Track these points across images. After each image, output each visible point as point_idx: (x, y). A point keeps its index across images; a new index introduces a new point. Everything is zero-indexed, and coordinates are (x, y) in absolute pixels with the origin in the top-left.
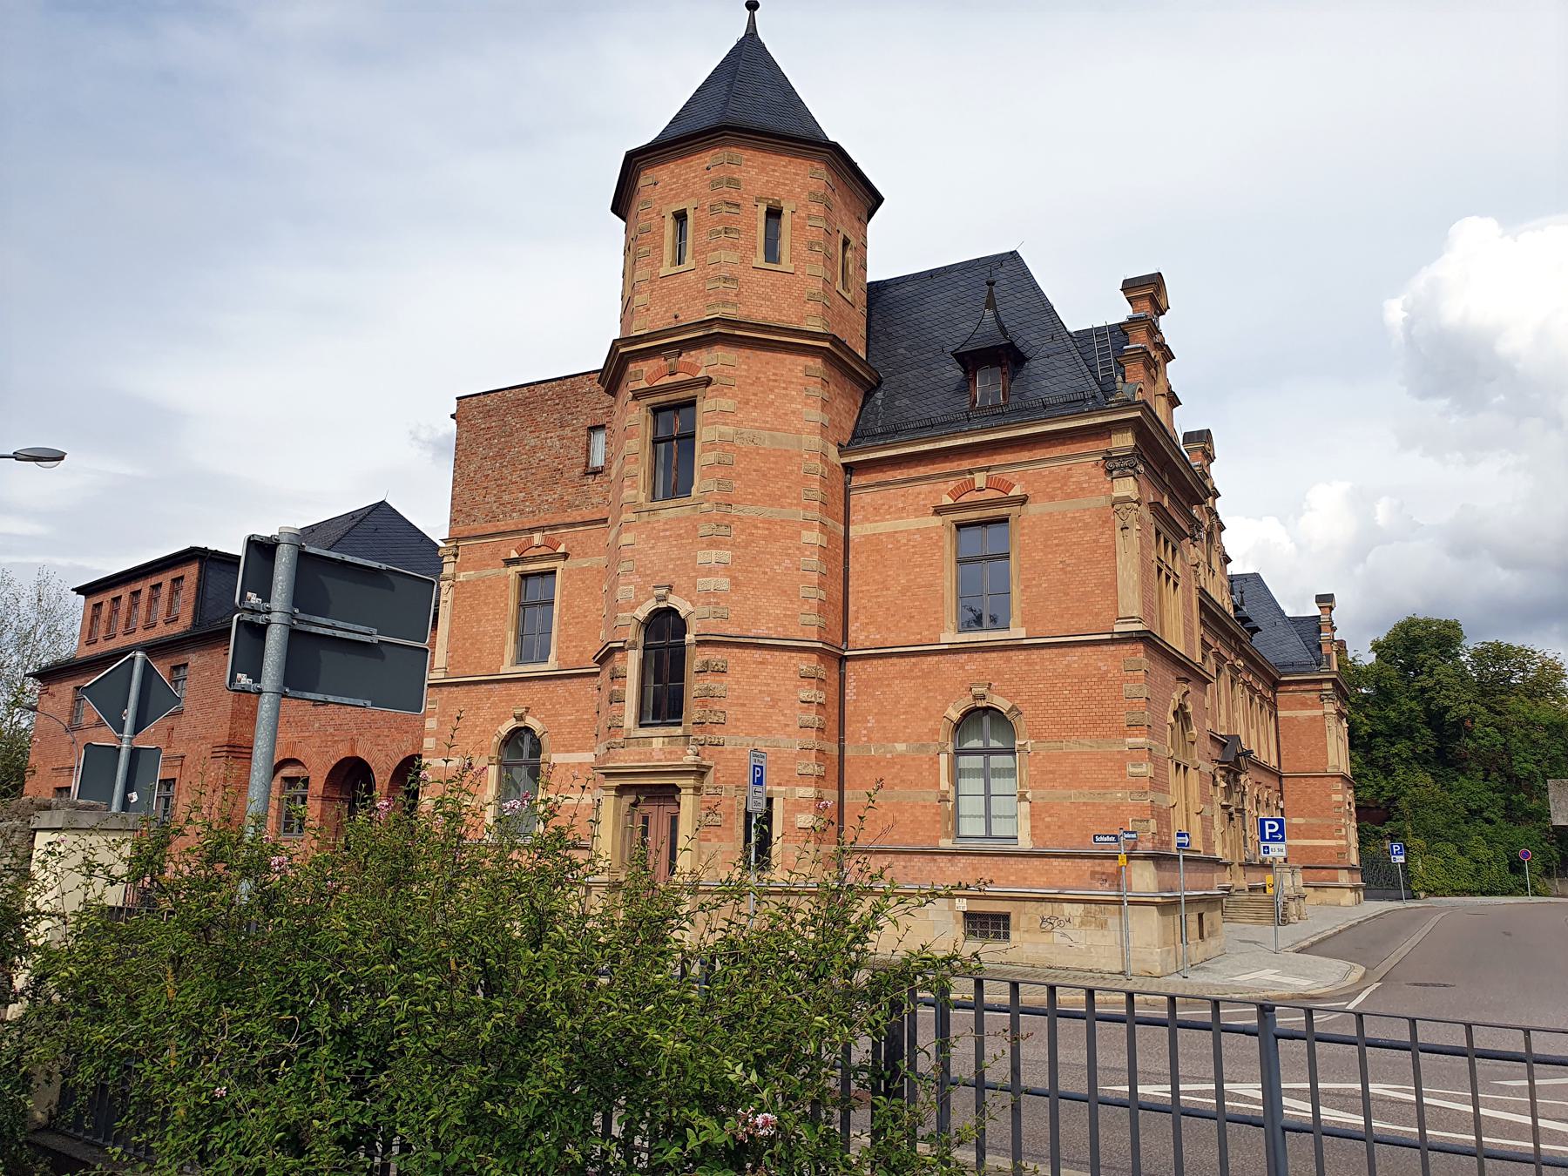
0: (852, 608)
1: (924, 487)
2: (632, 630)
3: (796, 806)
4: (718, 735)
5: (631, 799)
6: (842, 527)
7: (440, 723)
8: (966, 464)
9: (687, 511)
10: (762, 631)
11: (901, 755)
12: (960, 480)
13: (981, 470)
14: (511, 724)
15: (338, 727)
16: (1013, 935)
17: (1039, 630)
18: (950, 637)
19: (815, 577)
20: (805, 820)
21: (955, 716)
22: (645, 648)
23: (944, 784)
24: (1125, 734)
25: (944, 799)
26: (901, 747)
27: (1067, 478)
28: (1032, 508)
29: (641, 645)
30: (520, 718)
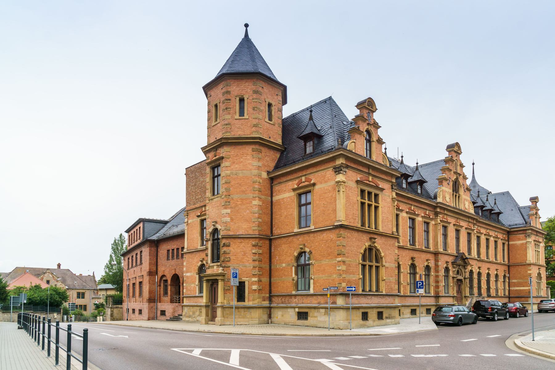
0: (274, 223)
1: (290, 183)
2: (209, 235)
3: (253, 283)
4: (228, 264)
5: (210, 283)
6: (270, 198)
7: (187, 264)
8: (300, 174)
9: (219, 199)
10: (241, 233)
11: (284, 267)
12: (299, 179)
13: (303, 176)
14: (200, 263)
15: (172, 266)
16: (309, 318)
17: (317, 226)
18: (296, 230)
19: (257, 215)
20: (255, 287)
21: (296, 254)
22: (213, 240)
23: (294, 275)
24: (336, 257)
25: (293, 280)
26: (284, 265)
27: (325, 176)
28: (317, 187)
29: (211, 239)
30: (202, 261)
